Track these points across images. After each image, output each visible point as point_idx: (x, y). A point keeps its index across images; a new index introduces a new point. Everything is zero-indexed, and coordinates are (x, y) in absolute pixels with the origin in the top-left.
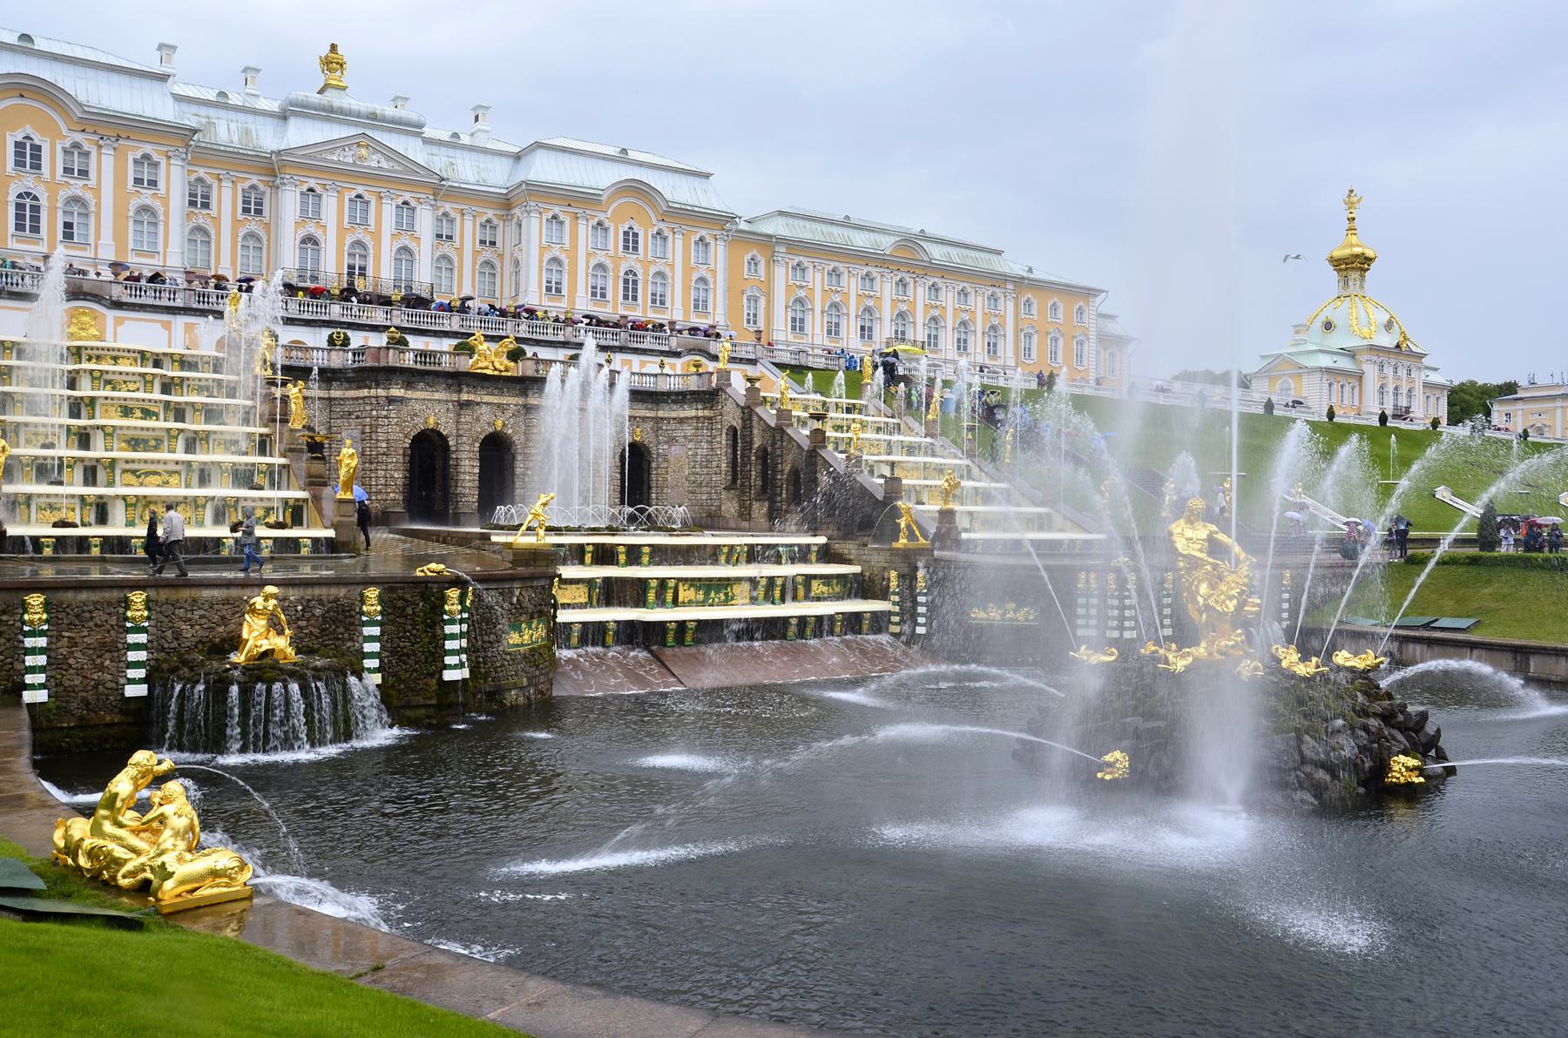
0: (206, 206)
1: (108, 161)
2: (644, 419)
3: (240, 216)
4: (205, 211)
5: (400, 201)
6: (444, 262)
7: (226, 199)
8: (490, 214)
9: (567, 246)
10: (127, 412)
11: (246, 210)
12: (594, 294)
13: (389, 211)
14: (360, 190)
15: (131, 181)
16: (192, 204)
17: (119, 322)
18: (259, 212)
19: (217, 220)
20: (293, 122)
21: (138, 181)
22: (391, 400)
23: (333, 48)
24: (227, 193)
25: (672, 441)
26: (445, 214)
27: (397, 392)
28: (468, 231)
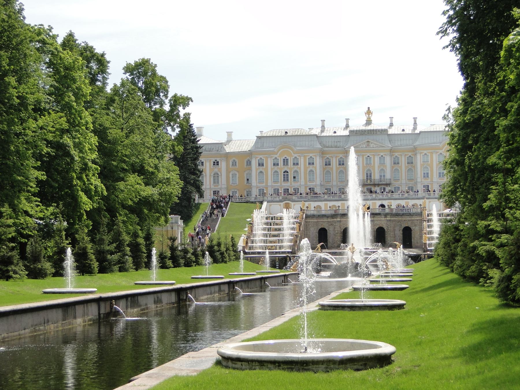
0: (330, 164)
1: (302, 160)
2: (409, 220)
3: (338, 166)
4: (329, 166)
5: (380, 156)
6: (395, 171)
7: (334, 163)
8: (410, 154)
9: (429, 163)
10: (276, 230)
11: (340, 164)
12: (440, 176)
13: (377, 159)
14: (368, 154)
15: (308, 164)
16: (326, 165)
17: (294, 205)
18: (343, 164)
19: (332, 169)
20: (352, 138)
21: (309, 164)
22: (338, 221)
23: (369, 108)
24: (334, 160)
25: (415, 225)
26: (396, 157)
27: (339, 219)
28: (403, 161)
